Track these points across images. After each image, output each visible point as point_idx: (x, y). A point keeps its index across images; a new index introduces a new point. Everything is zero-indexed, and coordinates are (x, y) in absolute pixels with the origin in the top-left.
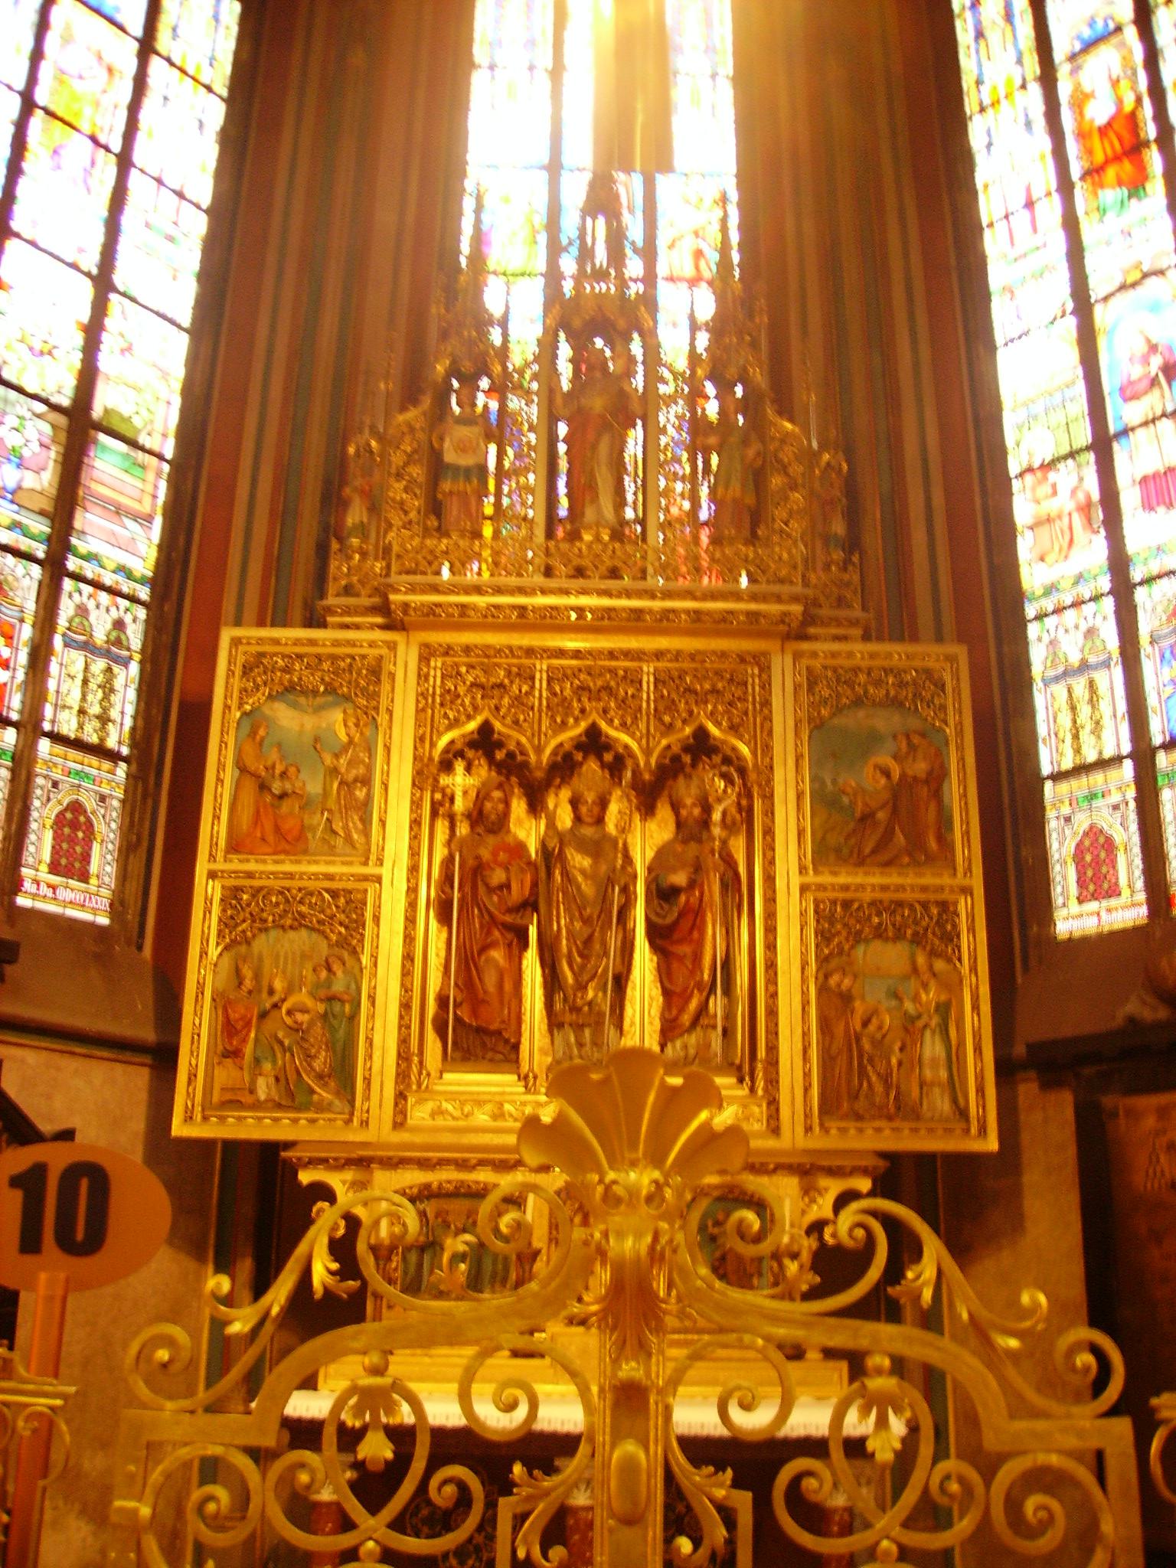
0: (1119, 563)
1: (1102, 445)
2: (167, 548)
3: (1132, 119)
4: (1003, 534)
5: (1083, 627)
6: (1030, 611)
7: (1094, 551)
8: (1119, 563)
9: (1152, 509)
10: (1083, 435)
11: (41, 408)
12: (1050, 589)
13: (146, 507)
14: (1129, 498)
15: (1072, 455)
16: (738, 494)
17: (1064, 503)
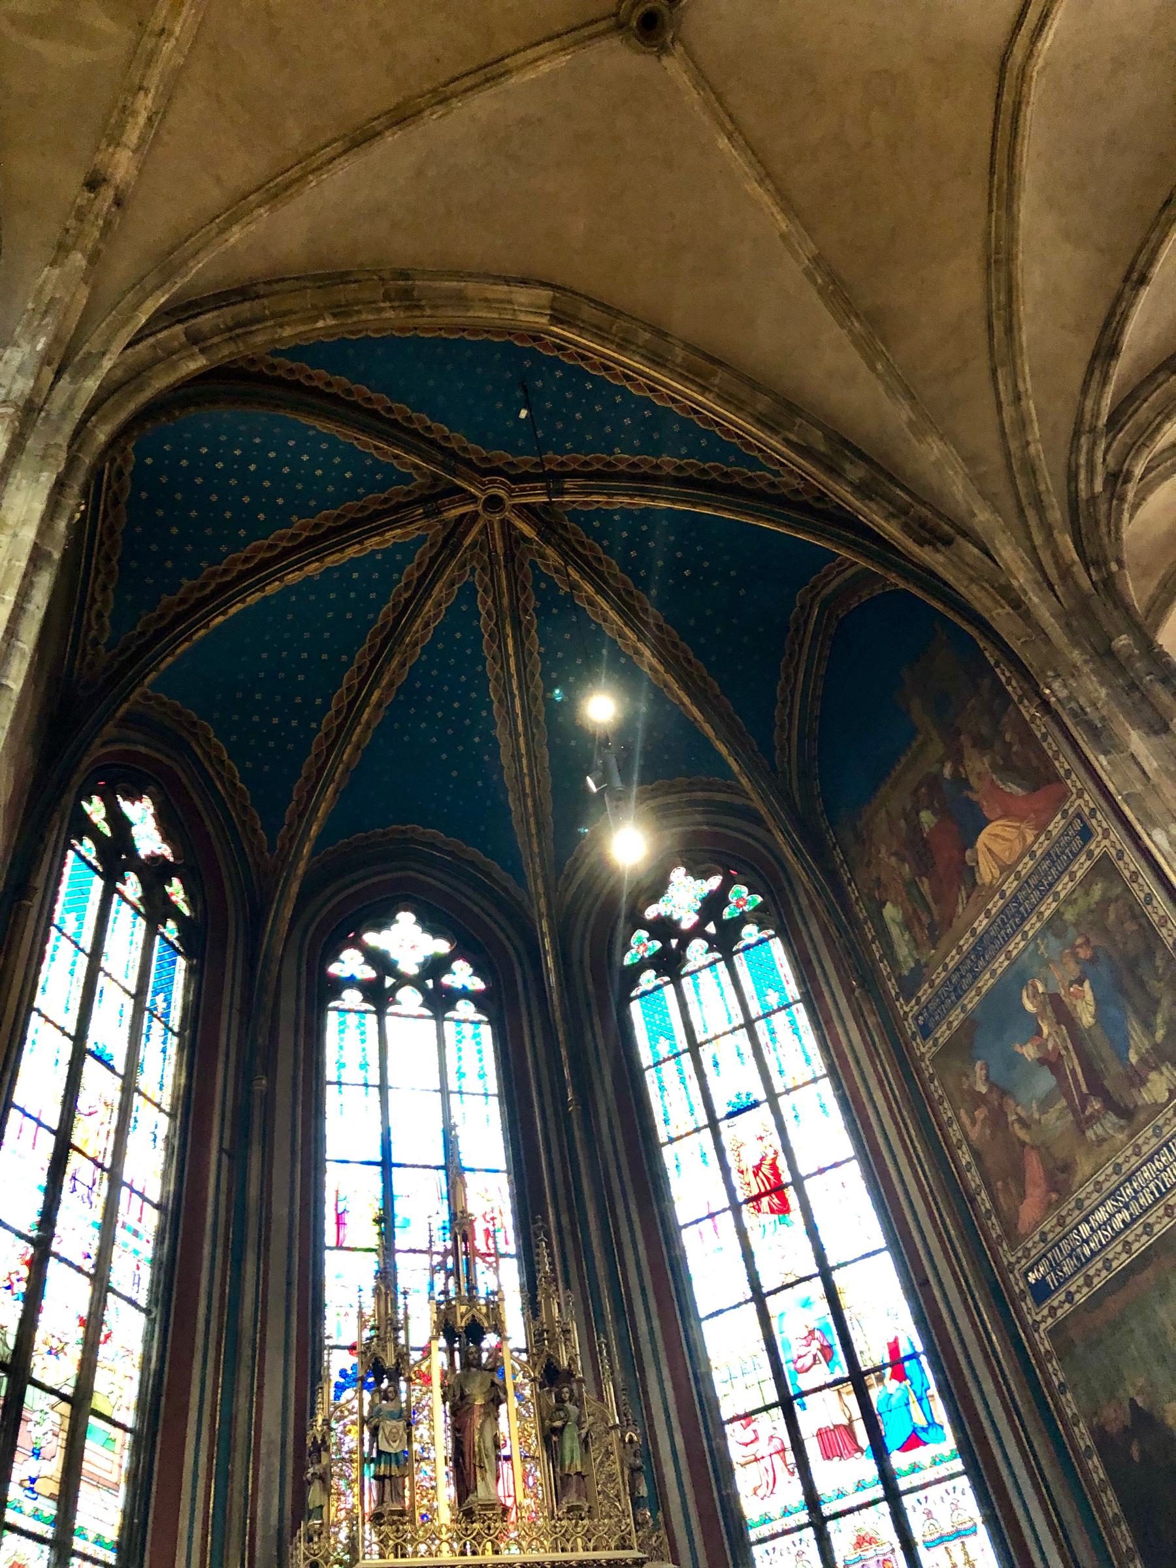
0: (812, 1501)
1: (787, 1403)
2: (128, 1515)
3: (774, 1167)
4: (724, 1471)
5: (794, 1550)
6: (753, 1535)
7: (793, 1492)
8: (812, 1501)
9: (829, 1458)
10: (773, 1397)
11: (54, 1399)
12: (767, 1519)
13: (113, 1478)
14: (812, 1448)
15: (766, 1408)
16: (579, 1469)
17: (763, 1448)
